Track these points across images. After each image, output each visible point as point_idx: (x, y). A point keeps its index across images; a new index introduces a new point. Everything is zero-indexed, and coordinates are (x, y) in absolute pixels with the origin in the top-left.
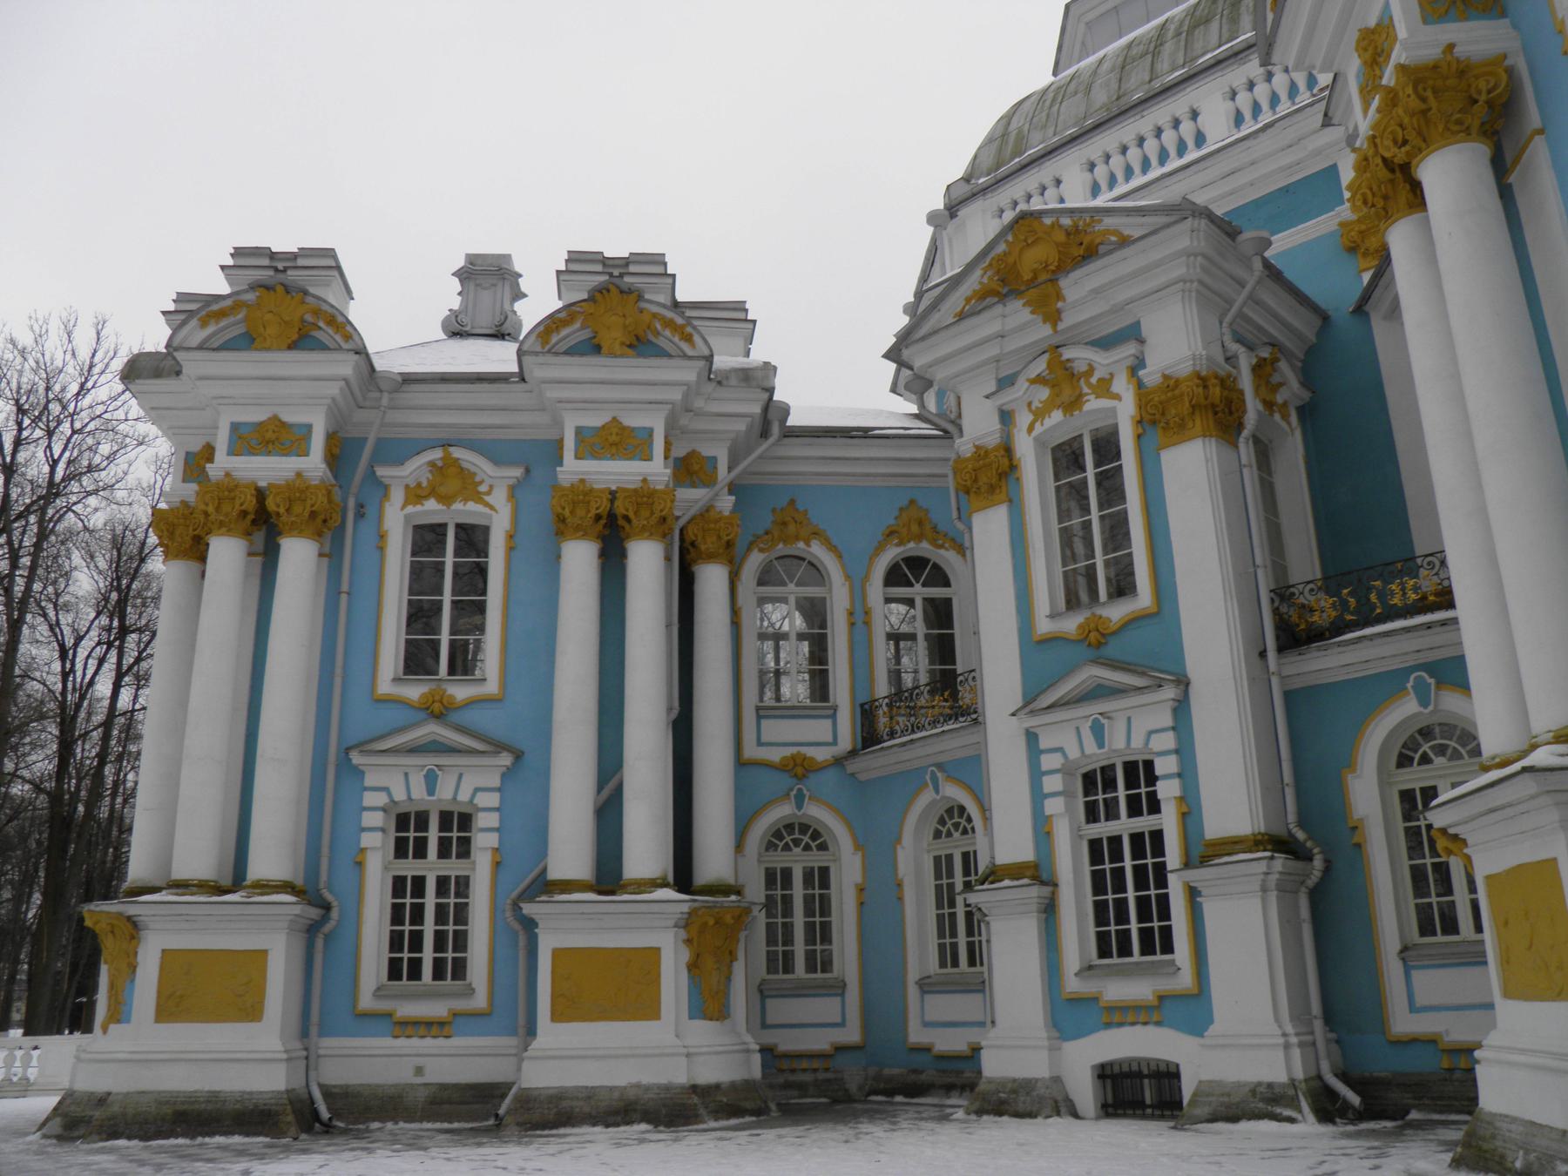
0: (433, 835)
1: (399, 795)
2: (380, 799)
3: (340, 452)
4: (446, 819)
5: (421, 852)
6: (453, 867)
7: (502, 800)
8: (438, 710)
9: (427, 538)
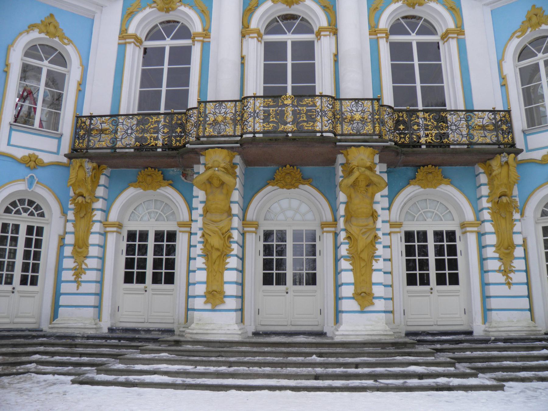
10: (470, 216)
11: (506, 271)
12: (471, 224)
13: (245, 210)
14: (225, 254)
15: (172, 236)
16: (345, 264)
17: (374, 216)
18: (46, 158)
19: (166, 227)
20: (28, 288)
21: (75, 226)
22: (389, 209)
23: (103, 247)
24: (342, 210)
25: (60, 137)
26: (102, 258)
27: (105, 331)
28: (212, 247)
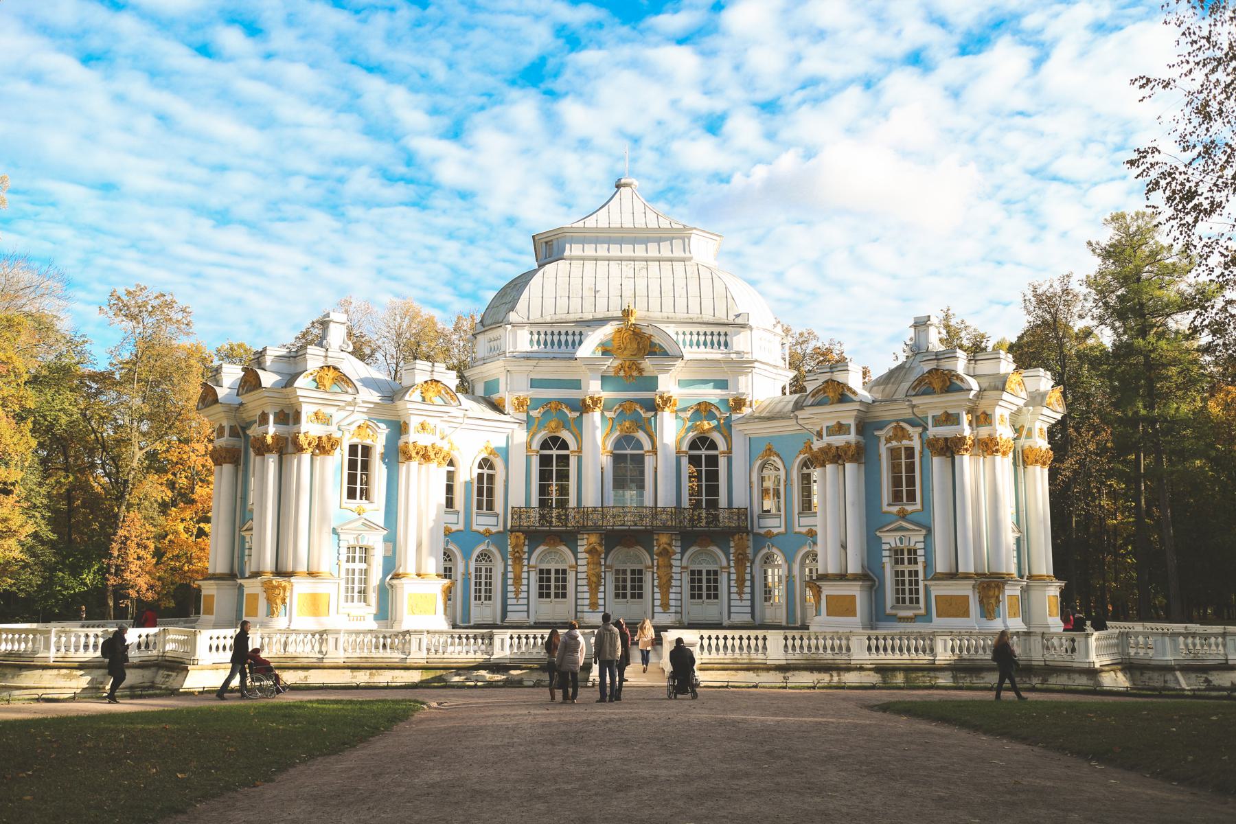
0: (906, 557)
1: (893, 545)
2: (887, 547)
4: (909, 551)
5: (903, 563)
6: (913, 568)
8: (903, 515)
10: (725, 563)
11: (740, 593)
12: (725, 568)
13: (605, 559)
14: (598, 585)
15: (564, 572)
16: (656, 590)
17: (671, 566)
18: (494, 530)
19: (561, 567)
20: (488, 602)
22: (681, 560)
23: (528, 579)
24: (655, 564)
25: (497, 515)
26: (528, 585)
27: (532, 623)
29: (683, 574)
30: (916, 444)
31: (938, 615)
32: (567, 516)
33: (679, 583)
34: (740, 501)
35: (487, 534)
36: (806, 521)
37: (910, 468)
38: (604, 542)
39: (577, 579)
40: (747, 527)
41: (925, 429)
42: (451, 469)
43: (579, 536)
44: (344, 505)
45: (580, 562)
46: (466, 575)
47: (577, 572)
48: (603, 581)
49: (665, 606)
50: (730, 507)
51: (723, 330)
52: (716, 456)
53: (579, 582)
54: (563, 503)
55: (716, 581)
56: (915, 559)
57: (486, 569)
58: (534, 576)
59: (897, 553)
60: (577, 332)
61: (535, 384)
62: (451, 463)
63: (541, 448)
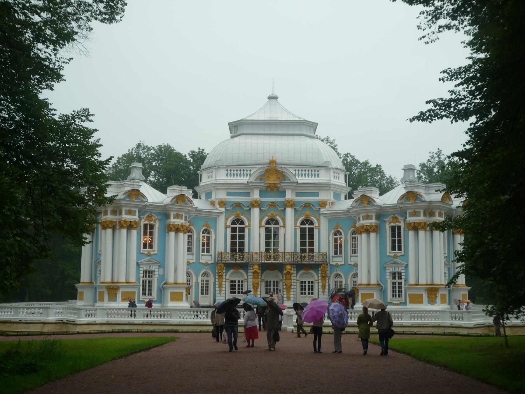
0: (397, 276)
1: (391, 271)
3: (378, 217)
4: (399, 273)
5: (395, 279)
6: (400, 281)
7: (405, 271)
9: (393, 229)
10: (316, 278)
11: (323, 292)
12: (317, 280)
13: (261, 276)
14: (257, 288)
15: (242, 282)
17: (291, 279)
18: (209, 262)
19: (241, 279)
20: (207, 296)
21: (218, 280)
22: (296, 276)
23: (225, 285)
24: (284, 277)
25: (211, 256)
26: (225, 288)
28: (255, 286)
29: (297, 283)
30: (402, 224)
31: (410, 302)
32: (243, 256)
33: (295, 287)
34: (324, 249)
35: (206, 264)
36: (353, 259)
37: (399, 235)
38: (260, 268)
39: (248, 285)
40: (327, 262)
41: (406, 218)
42: (190, 234)
43: (249, 265)
44: (142, 252)
45: (249, 277)
46: (197, 283)
47: (248, 282)
48: (260, 286)
49: (289, 298)
50: (319, 252)
51: (317, 169)
52: (313, 229)
53: (249, 287)
54: (242, 250)
55: (312, 286)
56: (401, 277)
57: (206, 280)
58: (228, 284)
59: (394, 274)
60: (248, 170)
61: (229, 194)
62: (190, 231)
63: (231, 224)
